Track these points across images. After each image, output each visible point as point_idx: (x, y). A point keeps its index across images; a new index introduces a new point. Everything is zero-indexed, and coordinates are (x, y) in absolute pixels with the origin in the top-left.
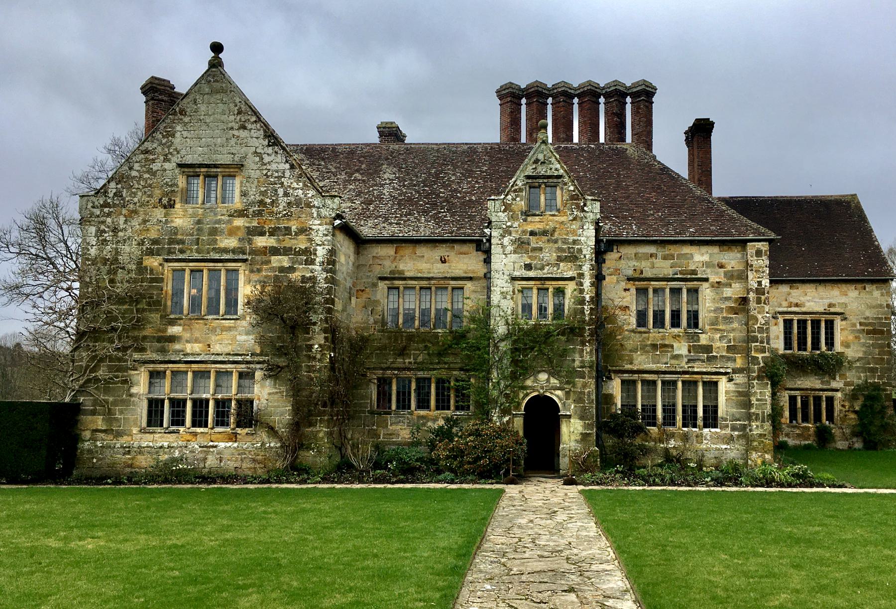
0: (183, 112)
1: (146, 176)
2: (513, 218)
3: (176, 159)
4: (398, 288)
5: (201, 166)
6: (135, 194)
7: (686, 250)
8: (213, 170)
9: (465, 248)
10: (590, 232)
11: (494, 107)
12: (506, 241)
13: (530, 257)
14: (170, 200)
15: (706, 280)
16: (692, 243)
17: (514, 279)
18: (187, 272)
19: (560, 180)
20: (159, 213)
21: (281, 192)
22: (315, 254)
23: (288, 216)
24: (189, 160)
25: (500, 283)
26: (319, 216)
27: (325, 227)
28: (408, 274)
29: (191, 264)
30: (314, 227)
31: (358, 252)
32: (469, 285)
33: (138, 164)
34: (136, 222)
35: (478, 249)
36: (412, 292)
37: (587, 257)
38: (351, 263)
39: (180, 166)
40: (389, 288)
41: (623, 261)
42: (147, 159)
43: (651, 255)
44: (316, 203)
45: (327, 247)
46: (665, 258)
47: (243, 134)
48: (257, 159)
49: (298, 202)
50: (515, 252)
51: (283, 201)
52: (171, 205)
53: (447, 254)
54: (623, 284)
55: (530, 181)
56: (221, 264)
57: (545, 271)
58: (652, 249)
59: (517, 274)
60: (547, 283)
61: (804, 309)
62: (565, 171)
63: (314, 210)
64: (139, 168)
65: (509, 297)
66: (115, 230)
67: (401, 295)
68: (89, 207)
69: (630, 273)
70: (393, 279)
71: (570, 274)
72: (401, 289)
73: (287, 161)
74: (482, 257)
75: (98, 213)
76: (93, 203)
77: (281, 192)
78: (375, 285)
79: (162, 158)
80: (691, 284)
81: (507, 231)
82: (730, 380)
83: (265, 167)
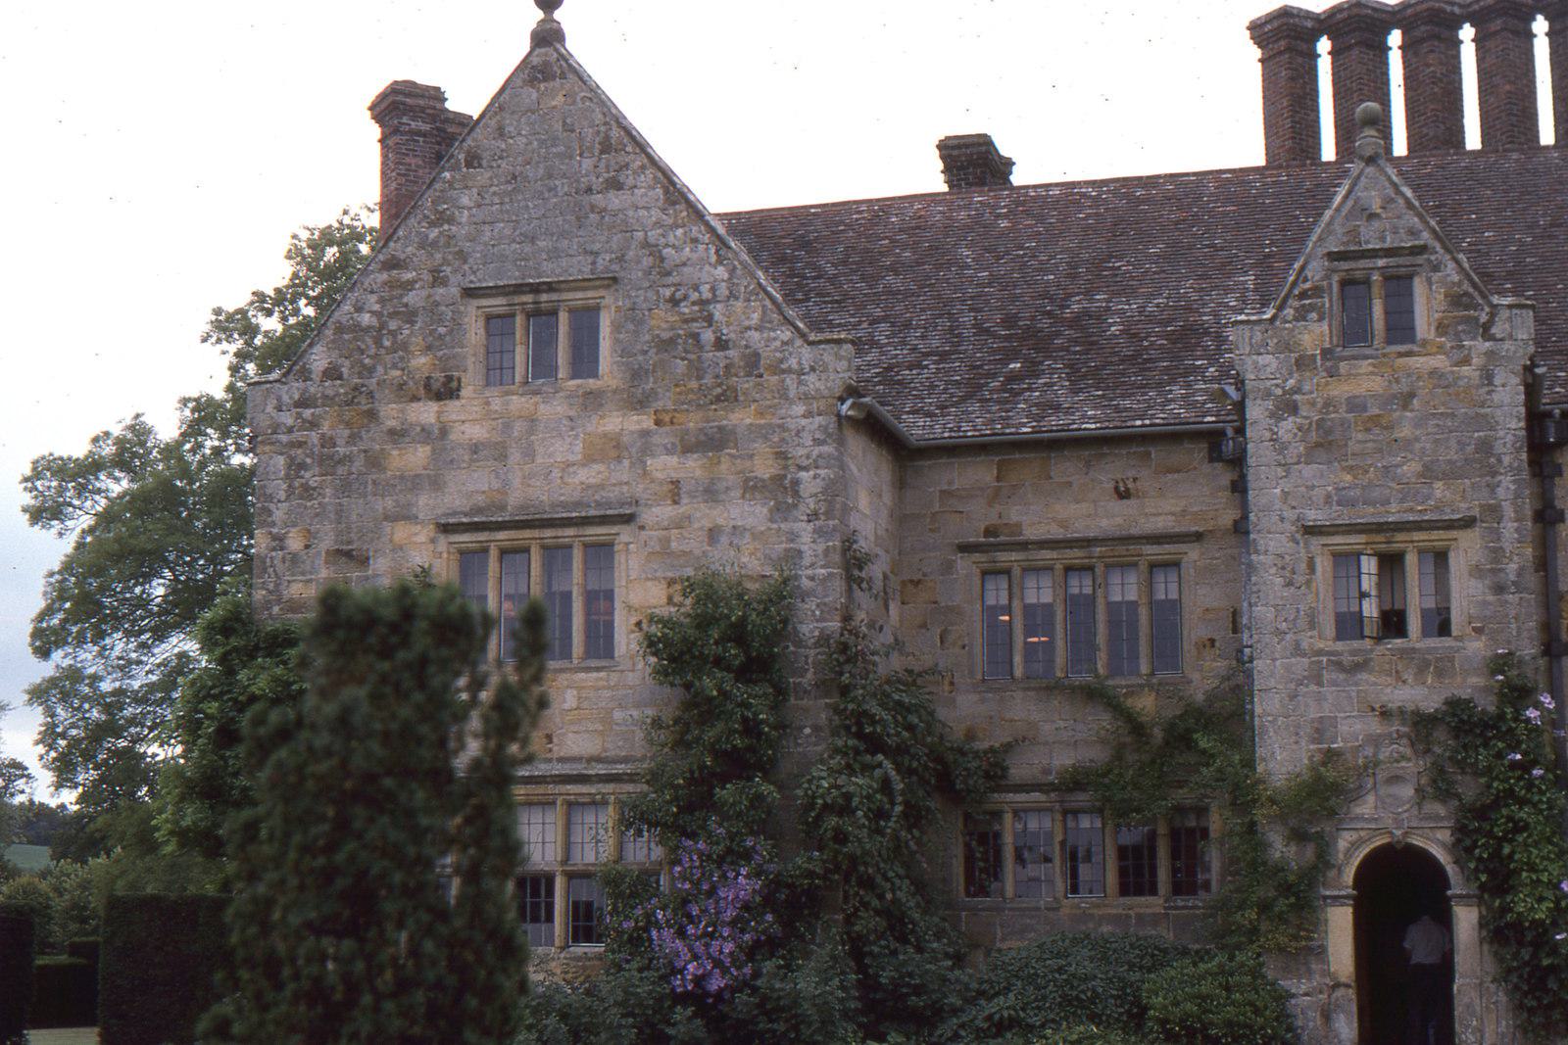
0: (473, 160)
1: (393, 325)
2: (1303, 363)
4: (1008, 572)
5: (519, 289)
6: (371, 370)
8: (544, 297)
9: (1178, 455)
10: (1509, 395)
11: (1247, 64)
12: (1288, 426)
13: (1350, 469)
14: (450, 379)
17: (1311, 531)
18: (494, 553)
19: (1420, 259)
20: (426, 413)
21: (708, 336)
22: (796, 494)
25: (1273, 541)
26: (806, 398)
27: (819, 420)
29: (502, 535)
30: (792, 424)
31: (901, 484)
32: (1192, 554)
33: (373, 298)
35: (1215, 454)
36: (1046, 581)
37: (1506, 460)
38: (885, 513)
39: (470, 293)
40: (985, 573)
42: (390, 285)
44: (793, 362)
45: (822, 472)
48: (647, 261)
49: (752, 361)
50: (1309, 458)
53: (1131, 473)
55: (1345, 265)
56: (571, 532)
57: (1394, 507)
60: (1400, 537)
62: (1434, 231)
63: (790, 381)
64: (377, 307)
65: (1300, 579)
66: (329, 462)
67: (1016, 590)
68: (269, 409)
70: (994, 549)
71: (1463, 509)
72: (1016, 571)
73: (720, 262)
74: (1226, 477)
75: (290, 422)
76: (279, 399)
77: (708, 336)
79: (427, 277)
83: (670, 280)
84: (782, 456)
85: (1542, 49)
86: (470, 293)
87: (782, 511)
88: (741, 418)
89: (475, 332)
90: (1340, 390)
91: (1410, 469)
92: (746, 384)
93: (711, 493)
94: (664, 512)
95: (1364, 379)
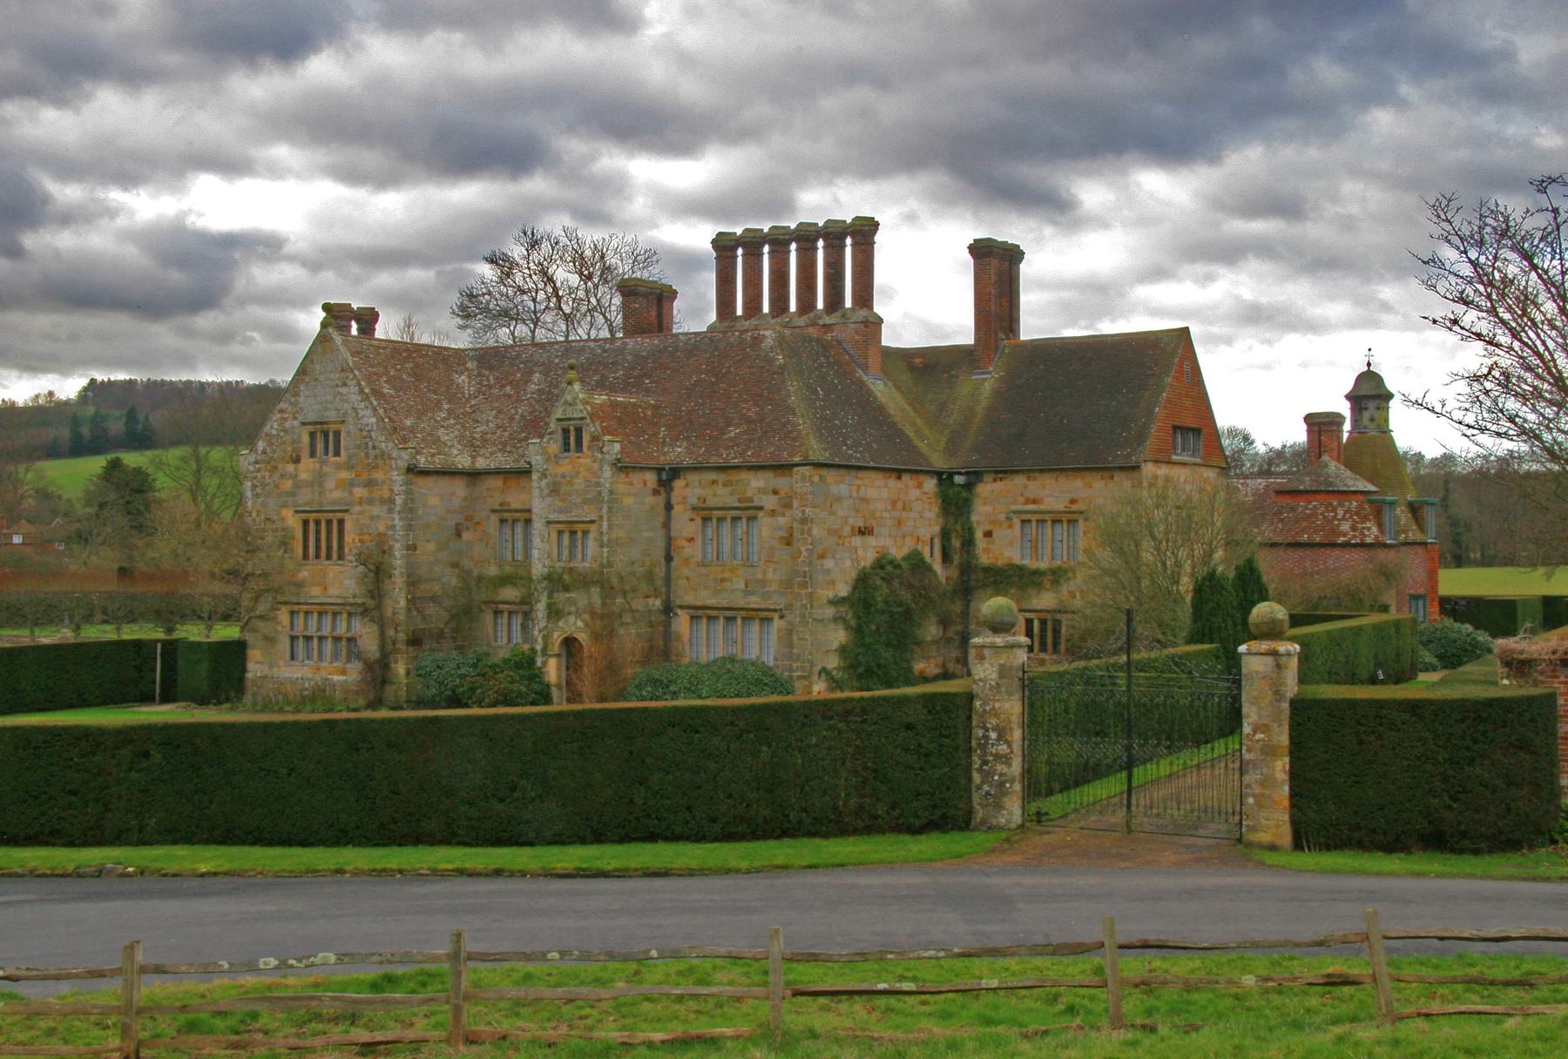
3: (301, 418)
5: (316, 423)
7: (744, 475)
15: (761, 508)
16: (750, 468)
20: (291, 468)
23: (376, 467)
24: (311, 418)
28: (513, 506)
34: (276, 477)
39: (303, 424)
41: (688, 490)
43: (714, 482)
46: (725, 485)
47: (344, 390)
49: (383, 454)
51: (372, 452)
52: (297, 460)
54: (688, 514)
58: (712, 476)
59: (552, 517)
61: (1041, 507)
66: (264, 485)
69: (693, 501)
78: (488, 518)
80: (747, 513)
81: (544, 476)
82: (782, 617)
84: (391, 490)
85: (848, 251)
86: (303, 424)
87: (391, 510)
88: (379, 475)
89: (306, 439)
90: (560, 471)
91: (579, 500)
92: (380, 462)
93: (371, 502)
94: (356, 509)
95: (565, 467)
